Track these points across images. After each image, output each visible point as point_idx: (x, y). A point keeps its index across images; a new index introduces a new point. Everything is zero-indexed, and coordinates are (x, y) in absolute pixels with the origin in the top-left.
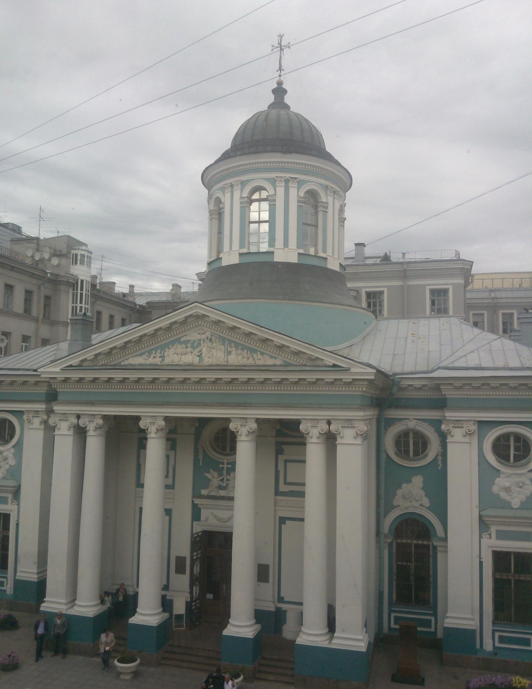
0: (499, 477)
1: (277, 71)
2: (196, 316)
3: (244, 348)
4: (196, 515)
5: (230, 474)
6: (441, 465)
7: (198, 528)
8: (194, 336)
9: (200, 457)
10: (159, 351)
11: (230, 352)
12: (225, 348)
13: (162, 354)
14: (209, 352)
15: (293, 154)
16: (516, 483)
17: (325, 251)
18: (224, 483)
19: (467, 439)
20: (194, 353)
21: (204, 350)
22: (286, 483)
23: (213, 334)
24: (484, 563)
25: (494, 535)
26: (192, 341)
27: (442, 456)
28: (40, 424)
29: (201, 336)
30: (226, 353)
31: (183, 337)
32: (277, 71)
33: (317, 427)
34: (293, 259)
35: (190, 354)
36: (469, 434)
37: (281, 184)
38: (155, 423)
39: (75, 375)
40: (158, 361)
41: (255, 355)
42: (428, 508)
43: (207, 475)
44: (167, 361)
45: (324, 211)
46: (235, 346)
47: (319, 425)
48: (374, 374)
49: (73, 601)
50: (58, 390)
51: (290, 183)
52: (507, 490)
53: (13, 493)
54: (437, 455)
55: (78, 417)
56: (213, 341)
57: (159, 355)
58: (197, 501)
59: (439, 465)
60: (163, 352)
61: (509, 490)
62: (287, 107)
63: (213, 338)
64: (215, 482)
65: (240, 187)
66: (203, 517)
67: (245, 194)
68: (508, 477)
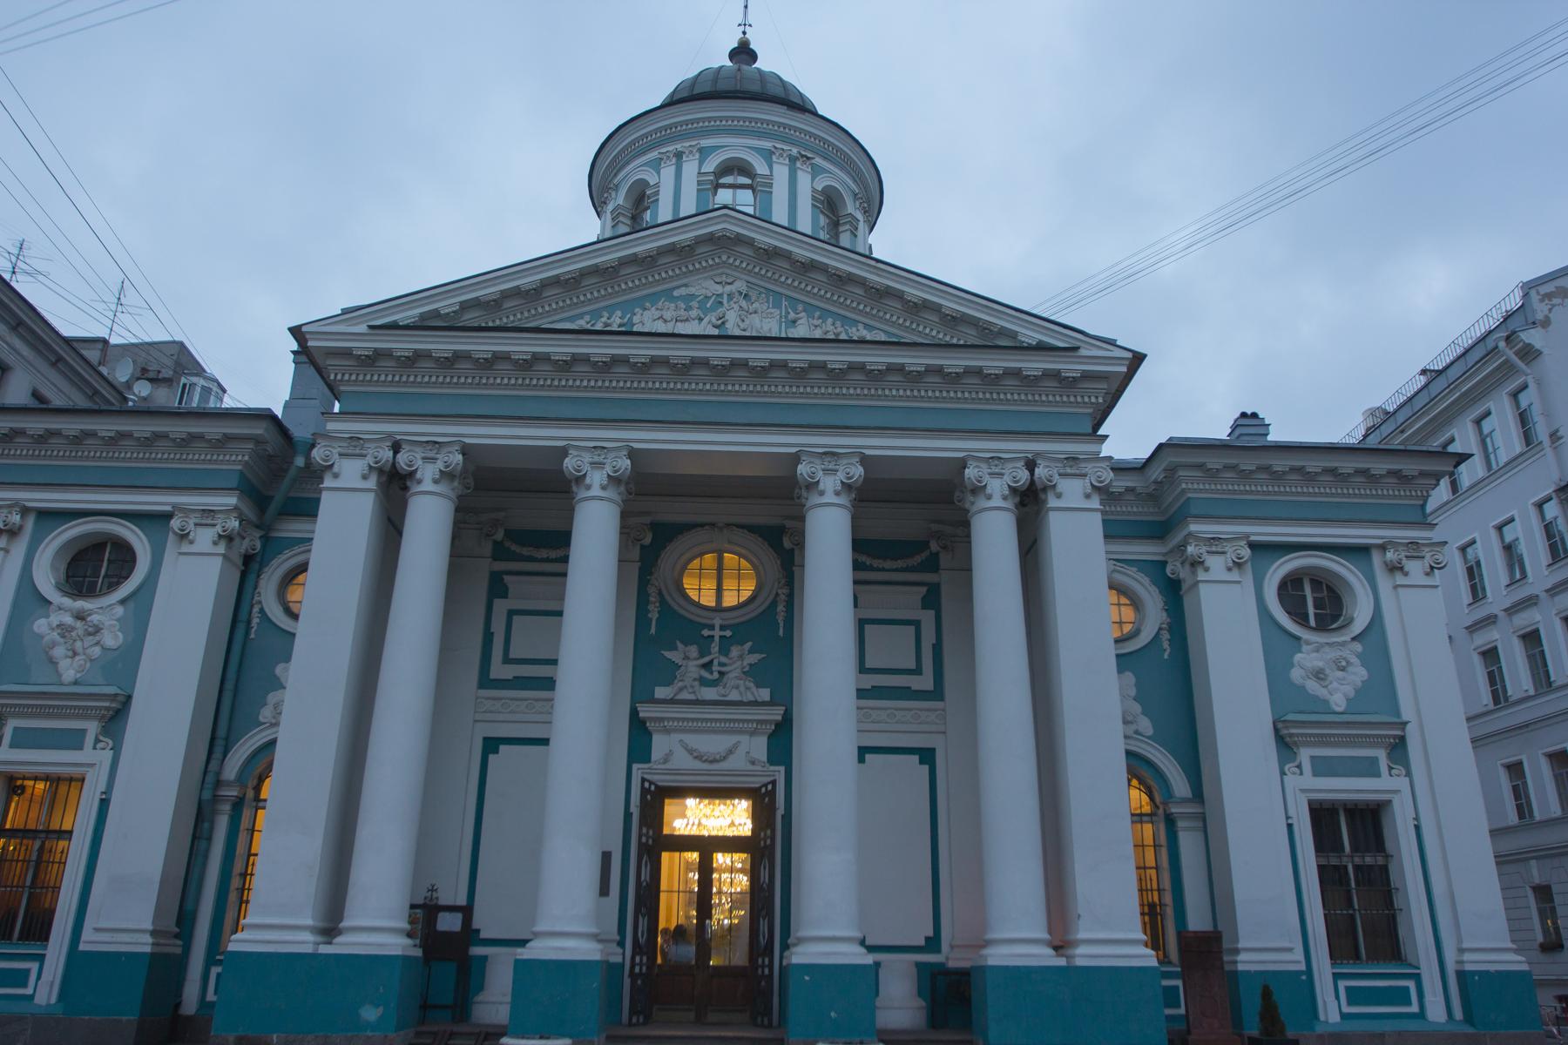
0: (1301, 652)
1: (740, 25)
2: (719, 238)
3: (825, 313)
5: (729, 650)
6: (1168, 651)
8: (706, 287)
9: (650, 615)
10: (619, 313)
11: (794, 322)
12: (781, 313)
13: (626, 320)
14: (743, 321)
15: (807, 114)
16: (1334, 662)
18: (712, 673)
19: (1235, 576)
20: (706, 320)
23: (749, 285)
24: (1296, 828)
25: (1307, 767)
26: (700, 298)
27: (1168, 631)
28: (215, 543)
29: (723, 287)
30: (783, 324)
31: (678, 287)
32: (740, 25)
33: (1003, 474)
35: (697, 321)
36: (1238, 565)
37: (781, 160)
38: (604, 464)
39: (403, 345)
41: (854, 329)
42: (1149, 738)
43: (668, 654)
45: (851, 231)
46: (804, 311)
47: (1006, 471)
48: (1128, 363)
49: (330, 930)
50: (342, 388)
51: (798, 164)
52: (1319, 675)
53: (103, 716)
54: (1160, 629)
55: (396, 447)
56: (753, 299)
57: (618, 321)
58: (645, 711)
59: (1165, 650)
60: (629, 316)
61: (1322, 676)
63: (754, 296)
64: (692, 669)
65: (697, 156)
66: (657, 752)
67: (711, 166)
68: (1317, 651)
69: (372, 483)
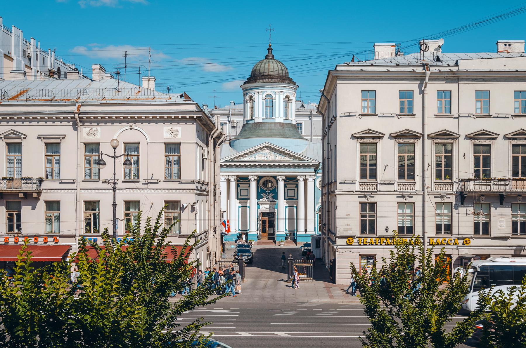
4: (258, 208)
17: (291, 118)
21: (268, 156)
22: (287, 196)
34: (282, 121)
39: (228, 164)
40: (253, 159)
44: (257, 159)
67: (264, 97)
69: (226, 180)
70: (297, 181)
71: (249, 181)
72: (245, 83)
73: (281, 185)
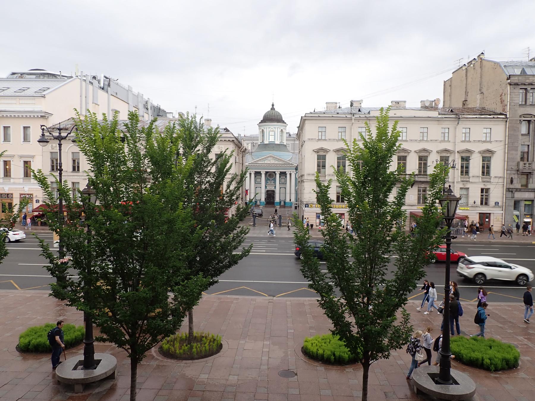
7: (266, 190)
8: (269, 159)
39: (250, 165)
62: (274, 109)
70: (286, 174)
71: (261, 174)
72: (260, 123)
73: (278, 176)
